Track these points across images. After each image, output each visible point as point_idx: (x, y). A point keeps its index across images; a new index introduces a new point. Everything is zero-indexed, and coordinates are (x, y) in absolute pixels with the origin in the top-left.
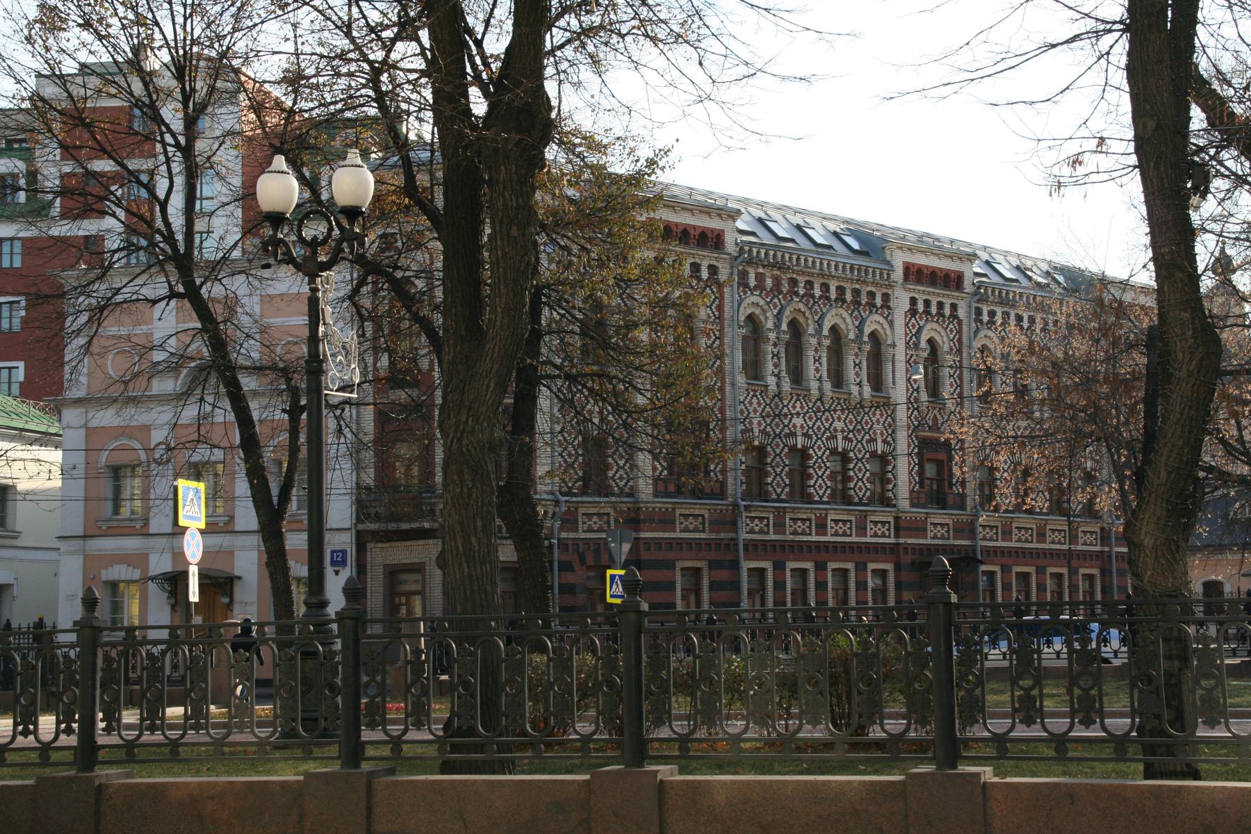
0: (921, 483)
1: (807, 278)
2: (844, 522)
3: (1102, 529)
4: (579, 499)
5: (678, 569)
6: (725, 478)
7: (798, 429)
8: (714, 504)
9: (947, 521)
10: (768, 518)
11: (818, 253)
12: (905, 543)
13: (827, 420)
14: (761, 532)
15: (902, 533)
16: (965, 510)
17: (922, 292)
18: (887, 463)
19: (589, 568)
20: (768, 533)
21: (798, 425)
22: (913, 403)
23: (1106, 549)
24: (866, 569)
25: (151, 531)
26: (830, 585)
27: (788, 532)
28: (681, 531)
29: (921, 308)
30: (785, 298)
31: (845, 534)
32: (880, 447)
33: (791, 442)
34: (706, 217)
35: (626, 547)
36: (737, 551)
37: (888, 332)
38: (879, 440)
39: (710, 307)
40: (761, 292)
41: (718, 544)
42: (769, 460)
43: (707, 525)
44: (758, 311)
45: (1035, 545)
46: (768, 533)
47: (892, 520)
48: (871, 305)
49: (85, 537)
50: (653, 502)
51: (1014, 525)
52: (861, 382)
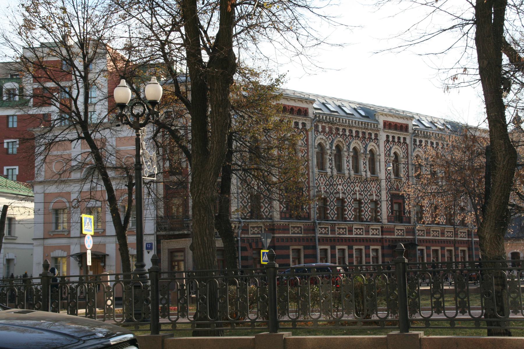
0: (392, 212)
1: (343, 128)
2: (360, 229)
3: (468, 231)
4: (249, 221)
5: (291, 249)
6: (310, 211)
7: (340, 190)
8: (306, 222)
9: (403, 228)
10: (328, 228)
11: (347, 117)
13: (352, 186)
14: (325, 233)
15: (384, 233)
17: (391, 133)
18: (378, 204)
19: (254, 249)
20: (328, 234)
21: (340, 189)
22: (388, 179)
23: (470, 239)
24: (369, 249)
25: (72, 236)
26: (354, 256)
27: (336, 233)
28: (292, 234)
29: (391, 139)
30: (334, 136)
31: (360, 234)
32: (375, 198)
33: (337, 196)
34: (300, 103)
35: (269, 240)
36: (315, 241)
37: (377, 150)
38: (374, 195)
39: (303, 140)
40: (324, 134)
41: (308, 239)
42: (328, 204)
43: (303, 231)
44: (323, 142)
46: (328, 234)
47: (380, 228)
48: (370, 138)
49: (44, 239)
50: (280, 222)
52: (366, 170)
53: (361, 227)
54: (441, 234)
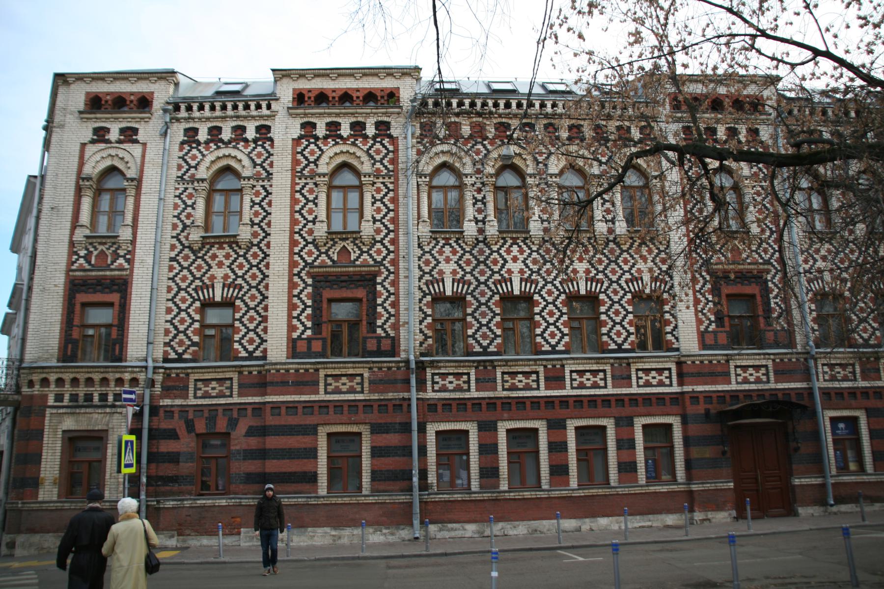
9: (764, 363)
12: (693, 391)
14: (458, 389)
15: (686, 379)
16: (796, 348)
18: (663, 302)
24: (632, 425)
27: (499, 388)
34: (376, 79)
40: (457, 141)
41: (383, 406)
43: (366, 385)
47: (673, 367)
53: (595, 367)
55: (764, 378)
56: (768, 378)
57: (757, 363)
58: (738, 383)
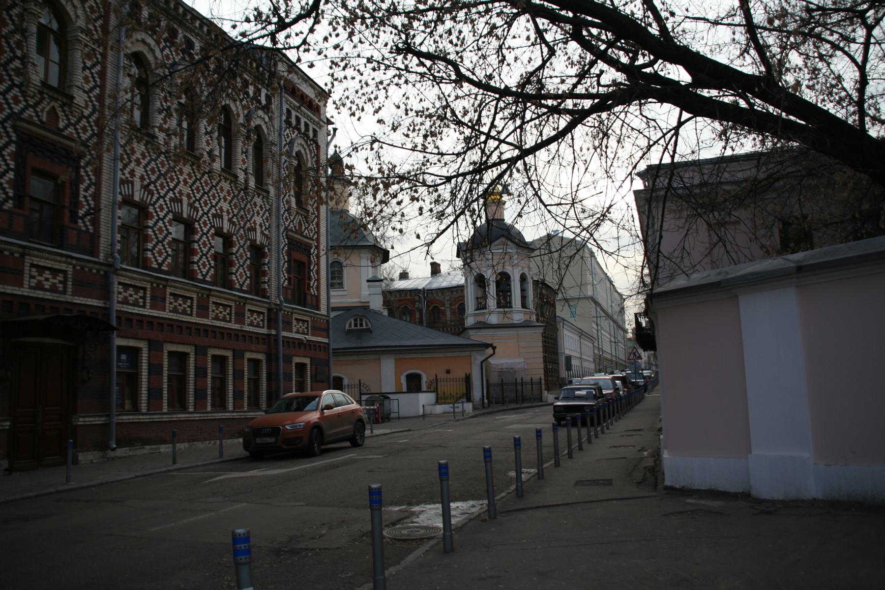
9: (63, 267)
16: (98, 257)
23: (273, 332)
45: (194, 319)
51: (169, 290)
54: (198, 307)
55: (60, 287)
56: (65, 288)
57: (57, 266)
58: (31, 287)
